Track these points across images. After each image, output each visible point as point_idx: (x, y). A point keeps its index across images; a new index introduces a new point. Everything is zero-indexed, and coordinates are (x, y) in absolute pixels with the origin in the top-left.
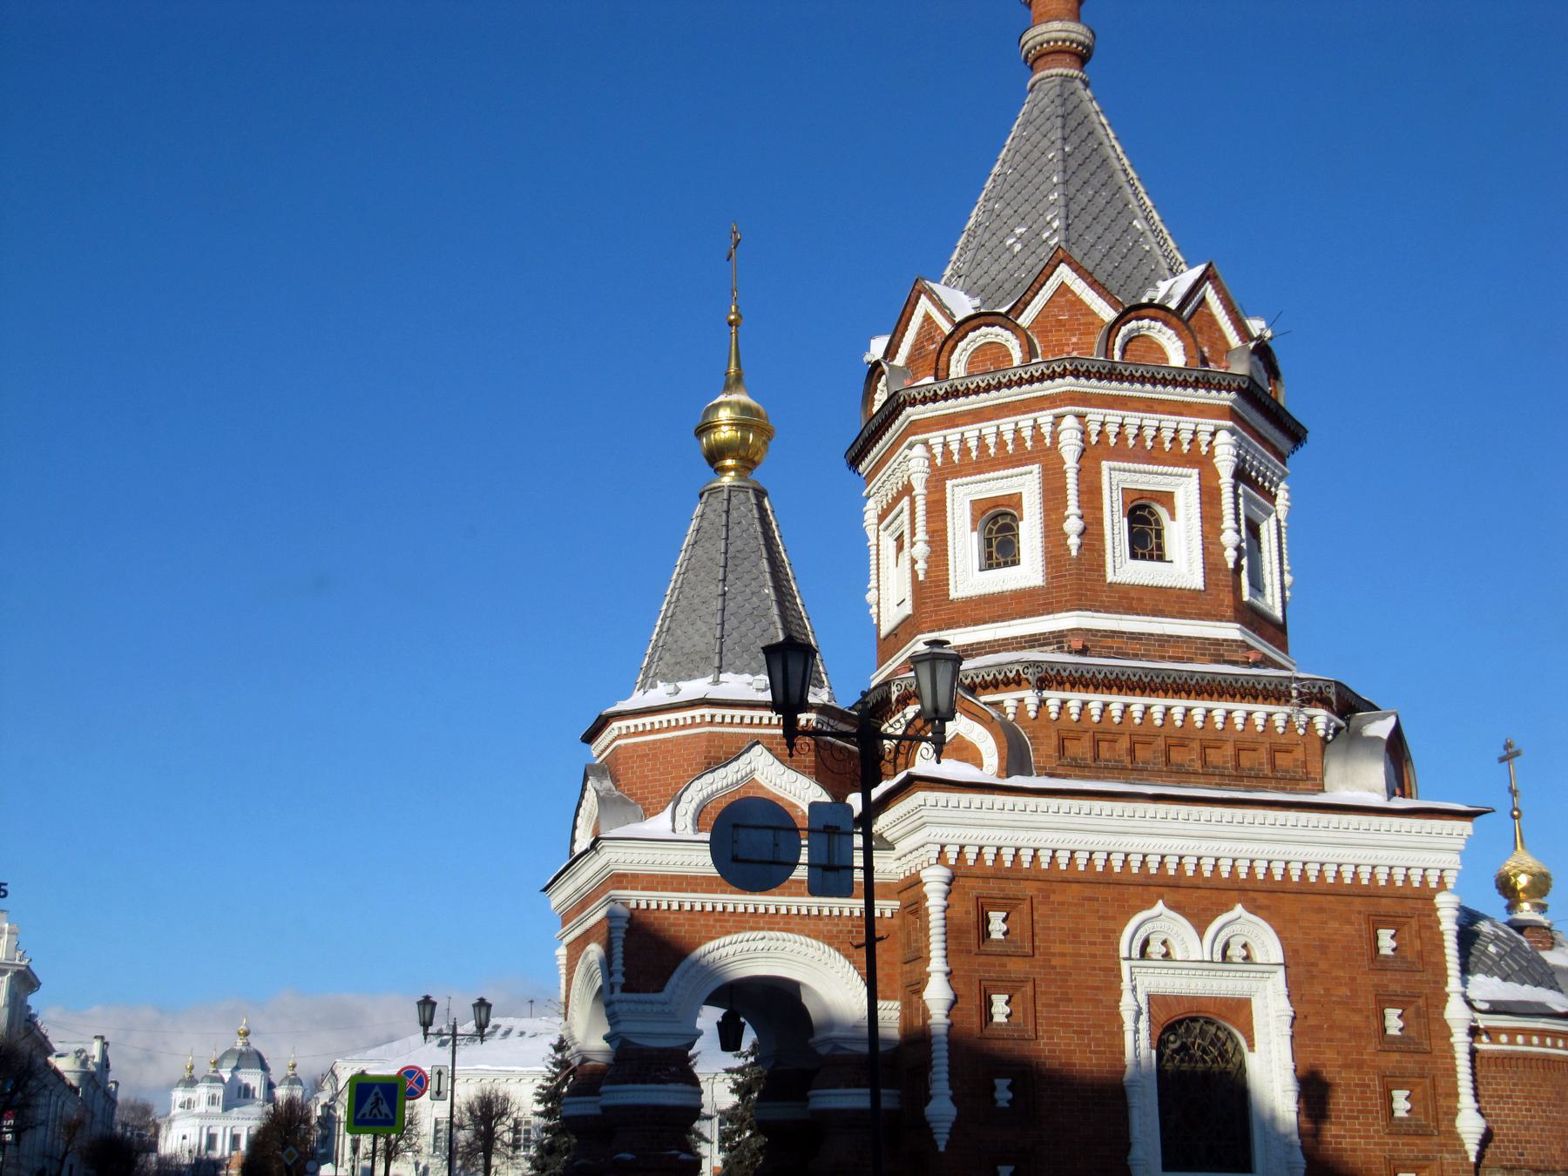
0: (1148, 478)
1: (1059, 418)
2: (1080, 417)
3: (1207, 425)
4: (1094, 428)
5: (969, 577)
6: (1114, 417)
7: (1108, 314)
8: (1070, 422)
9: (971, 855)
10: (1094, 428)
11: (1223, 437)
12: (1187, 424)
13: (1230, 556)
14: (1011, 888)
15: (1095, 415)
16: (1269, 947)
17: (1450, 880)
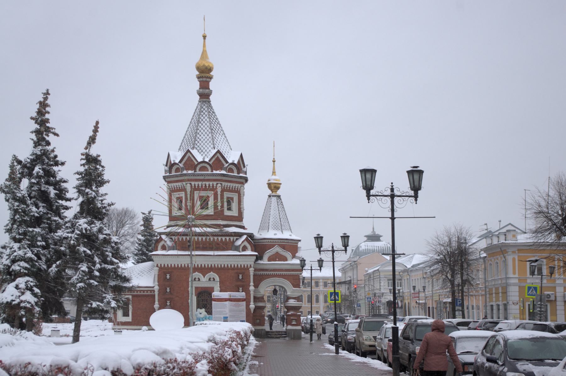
0: (203, 193)
1: (186, 184)
2: (191, 184)
3: (215, 183)
4: (193, 185)
5: (176, 213)
6: (196, 183)
7: (196, 163)
8: (189, 185)
9: (163, 266)
10: (193, 185)
11: (219, 185)
12: (211, 183)
13: (219, 207)
14: (170, 270)
15: (193, 183)
16: (217, 279)
17: (252, 266)
